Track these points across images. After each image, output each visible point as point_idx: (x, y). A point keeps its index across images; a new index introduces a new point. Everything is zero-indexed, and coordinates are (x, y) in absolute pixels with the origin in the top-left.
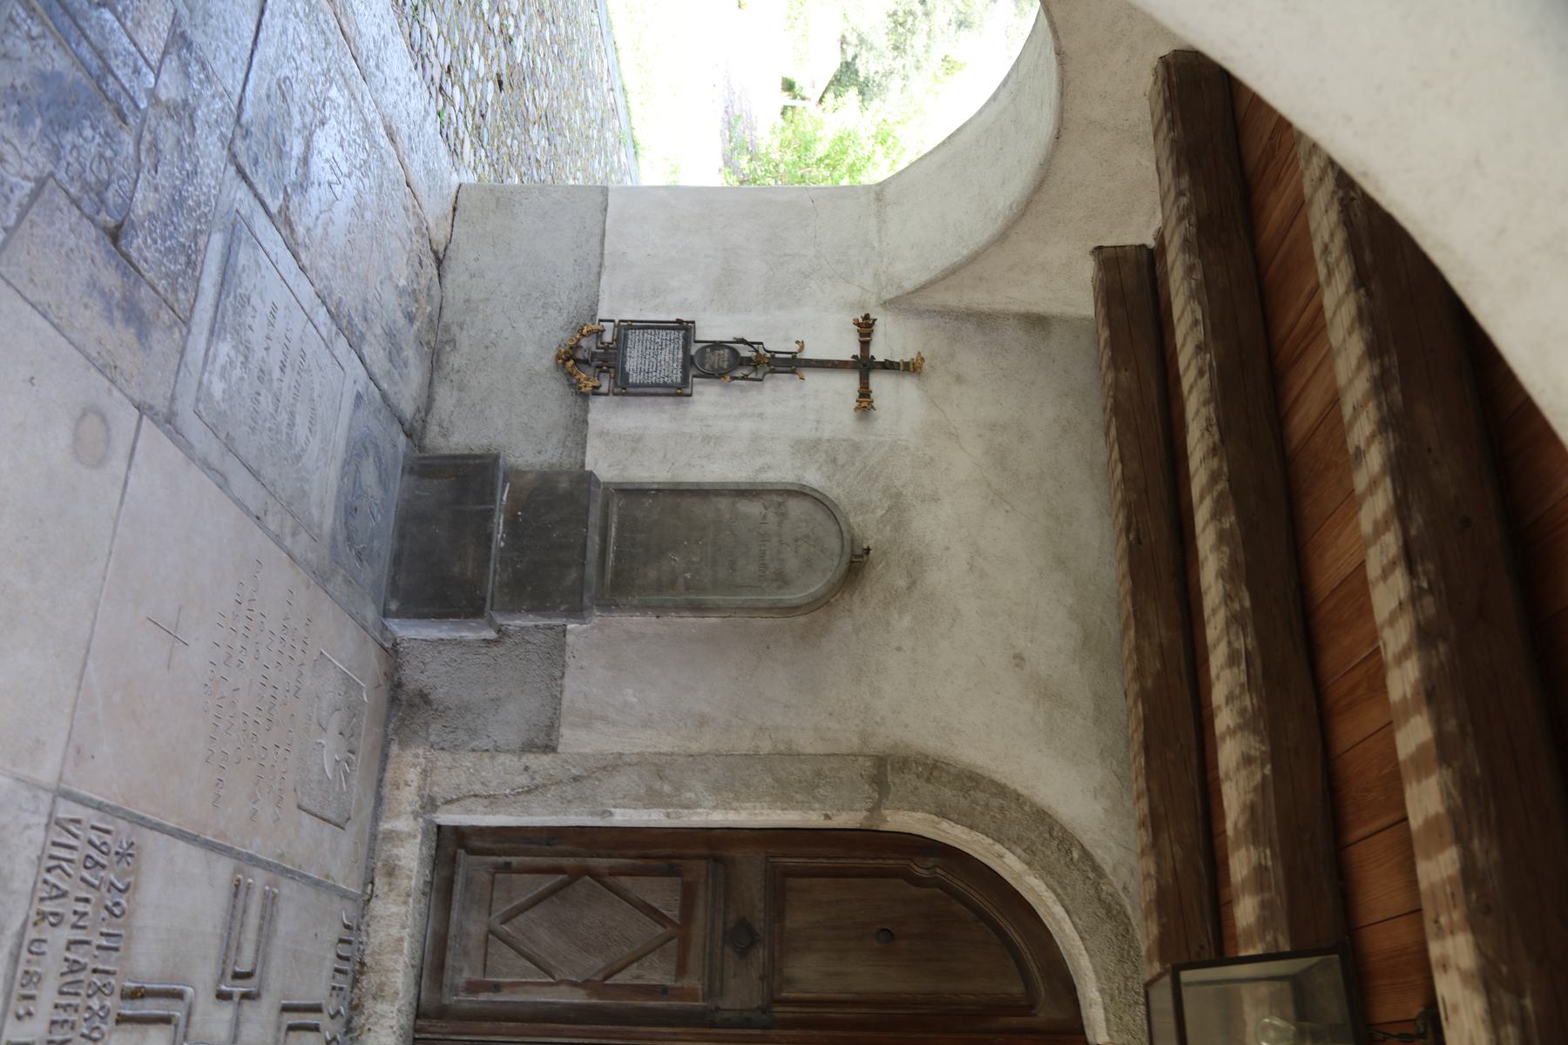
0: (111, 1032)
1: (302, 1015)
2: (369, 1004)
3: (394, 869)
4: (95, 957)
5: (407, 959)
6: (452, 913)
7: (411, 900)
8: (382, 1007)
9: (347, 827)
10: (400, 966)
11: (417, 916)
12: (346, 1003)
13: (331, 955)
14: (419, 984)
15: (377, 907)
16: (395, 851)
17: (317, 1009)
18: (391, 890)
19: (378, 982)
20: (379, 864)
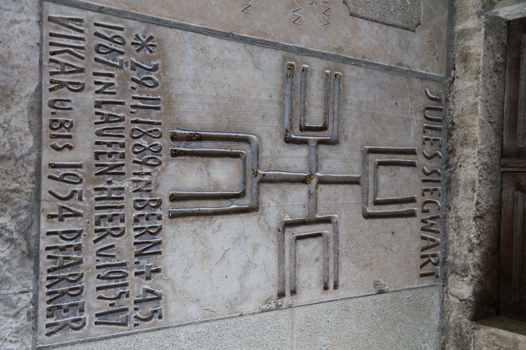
0: (167, 161)
1: (392, 156)
2: (459, 149)
3: (467, 56)
4: (132, 112)
5: (482, 117)
6: (521, 82)
7: (480, 76)
8: (467, 151)
9: (416, 30)
10: (477, 122)
11: (489, 87)
12: (443, 149)
13: (419, 117)
14: (499, 133)
15: (459, 84)
16: (467, 44)
17: (412, 152)
18: (466, 72)
19: (463, 134)
20: (457, 55)
